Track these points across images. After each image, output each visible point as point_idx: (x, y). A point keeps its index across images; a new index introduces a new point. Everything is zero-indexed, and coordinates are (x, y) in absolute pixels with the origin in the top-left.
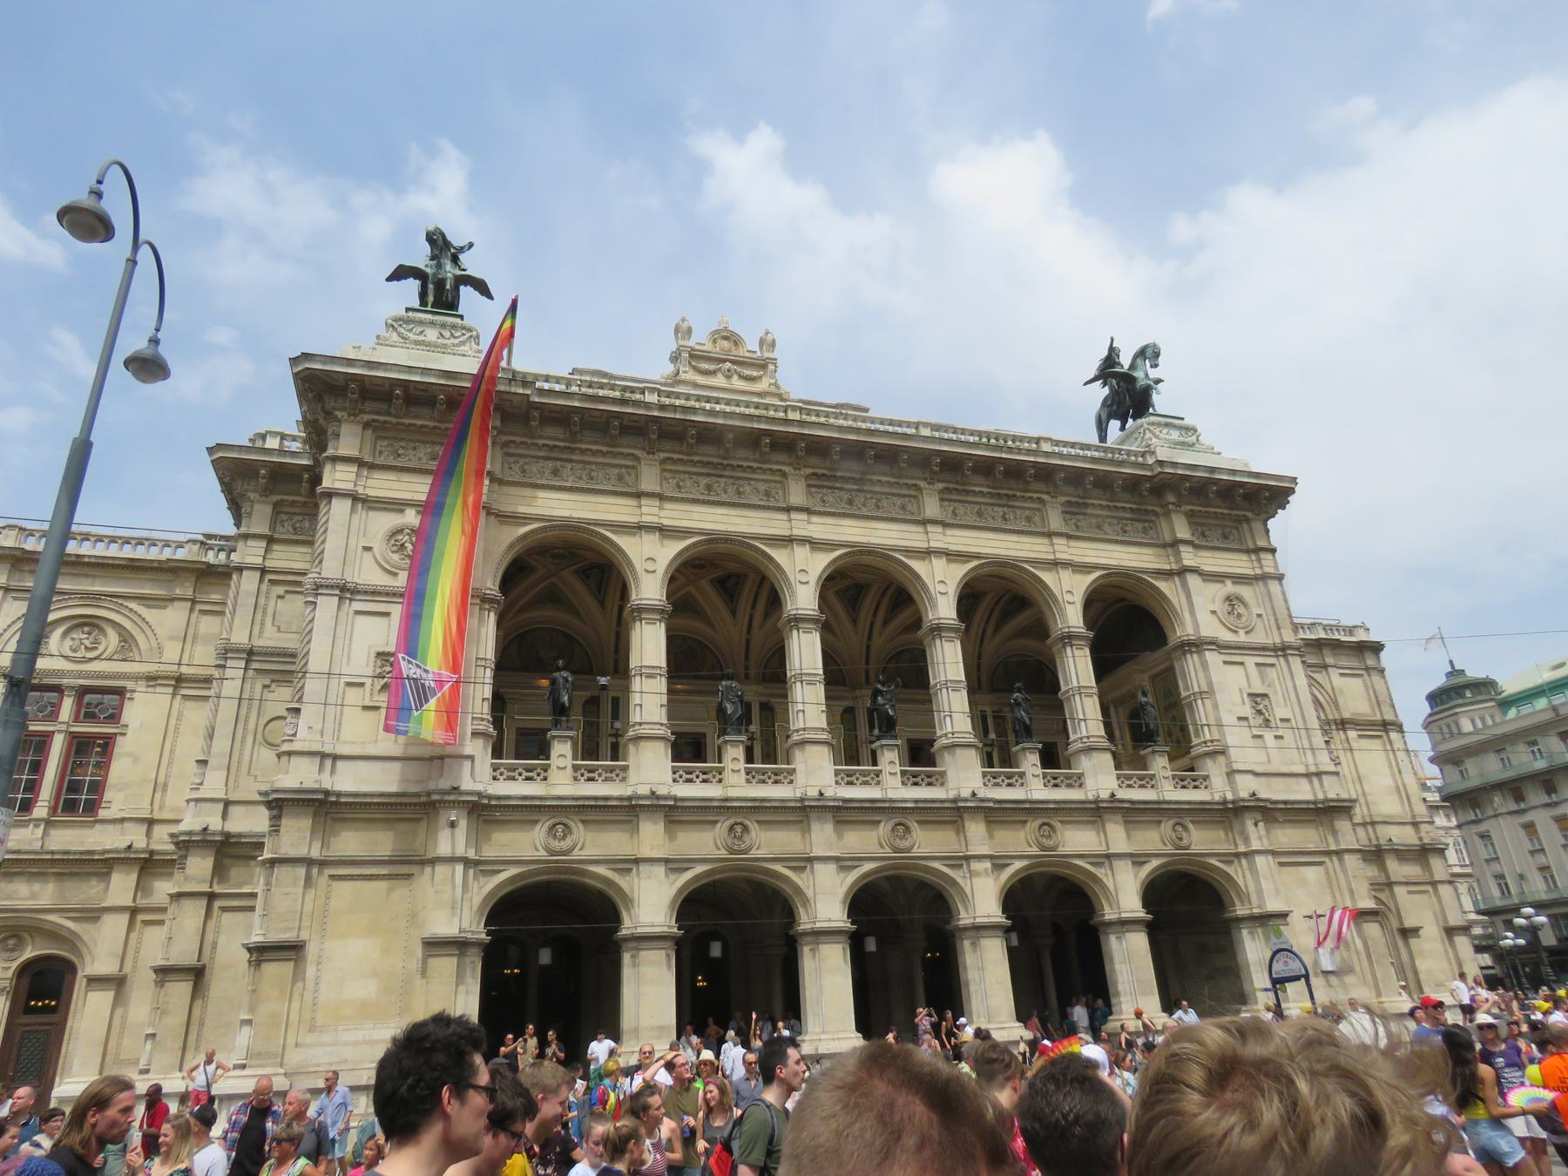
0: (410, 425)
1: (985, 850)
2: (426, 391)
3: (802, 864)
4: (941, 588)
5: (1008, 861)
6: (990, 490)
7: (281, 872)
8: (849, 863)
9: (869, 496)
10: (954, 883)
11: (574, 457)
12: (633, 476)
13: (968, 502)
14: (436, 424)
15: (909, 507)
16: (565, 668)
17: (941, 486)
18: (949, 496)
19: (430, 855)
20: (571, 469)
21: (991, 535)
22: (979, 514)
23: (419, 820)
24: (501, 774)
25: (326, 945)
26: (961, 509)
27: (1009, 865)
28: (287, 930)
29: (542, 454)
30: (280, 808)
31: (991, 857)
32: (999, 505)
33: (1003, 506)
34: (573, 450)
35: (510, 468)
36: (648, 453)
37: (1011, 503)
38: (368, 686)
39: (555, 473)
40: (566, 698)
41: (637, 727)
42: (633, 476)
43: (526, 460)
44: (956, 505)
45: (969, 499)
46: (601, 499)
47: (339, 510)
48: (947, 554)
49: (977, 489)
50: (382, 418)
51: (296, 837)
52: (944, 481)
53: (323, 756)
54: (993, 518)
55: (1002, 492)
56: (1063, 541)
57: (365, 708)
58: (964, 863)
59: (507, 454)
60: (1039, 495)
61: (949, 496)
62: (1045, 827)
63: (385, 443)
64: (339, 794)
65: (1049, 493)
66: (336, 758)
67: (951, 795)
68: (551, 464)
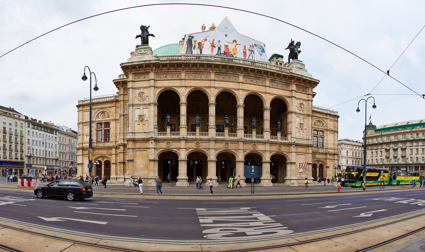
0: (140, 72)
1: (242, 149)
2: (141, 65)
3: (209, 150)
4: (241, 97)
5: (246, 151)
6: (254, 76)
7: (129, 150)
8: (217, 150)
9: (228, 76)
10: (236, 154)
11: (169, 73)
12: (180, 75)
13: (249, 78)
14: (144, 71)
15: (236, 79)
16: (169, 115)
17: (243, 74)
18: (245, 77)
19: (149, 147)
20: (169, 76)
21: (253, 86)
22: (252, 81)
23: (147, 142)
24: (159, 134)
25: (137, 160)
26: (248, 80)
27: (246, 151)
28: (131, 158)
29: (163, 73)
30: (128, 141)
31: (243, 150)
32: (256, 79)
33: (257, 79)
34: (169, 72)
35: (158, 77)
36: (183, 70)
37: (259, 79)
38: (138, 121)
39: (166, 77)
40: (169, 121)
41: (181, 126)
42: (180, 75)
43: (161, 75)
44: (247, 79)
45: (250, 77)
46: (174, 81)
47: (131, 90)
48: (243, 90)
49: (251, 75)
50: (135, 72)
51: (130, 145)
52: (244, 73)
53: (133, 133)
54: (254, 82)
55: (257, 76)
56: (268, 88)
57: (138, 125)
58: (238, 150)
59: (157, 74)
60: (265, 77)
61: (245, 77)
62: (254, 145)
63: (137, 76)
64: (136, 139)
65: (267, 77)
66: (135, 133)
67: (237, 138)
68: (165, 75)
